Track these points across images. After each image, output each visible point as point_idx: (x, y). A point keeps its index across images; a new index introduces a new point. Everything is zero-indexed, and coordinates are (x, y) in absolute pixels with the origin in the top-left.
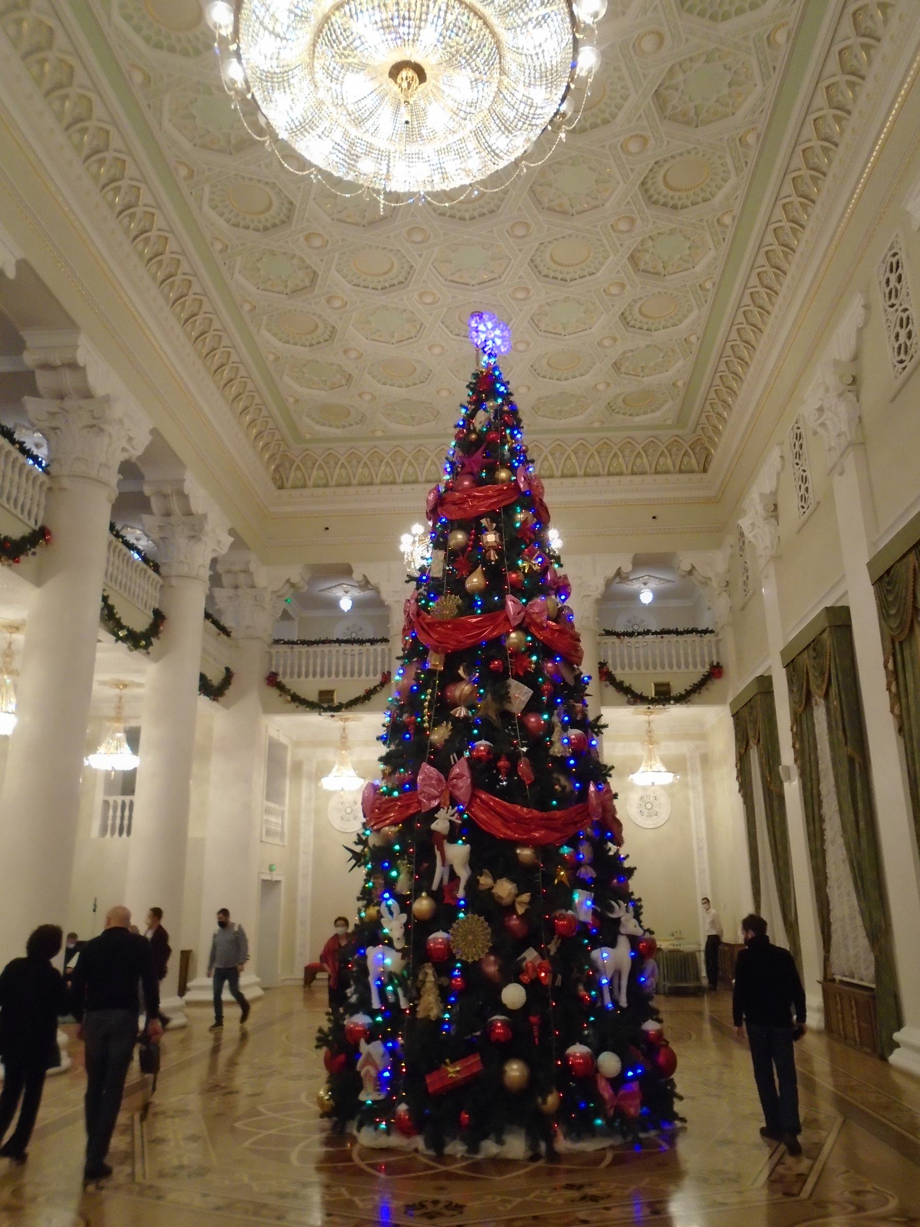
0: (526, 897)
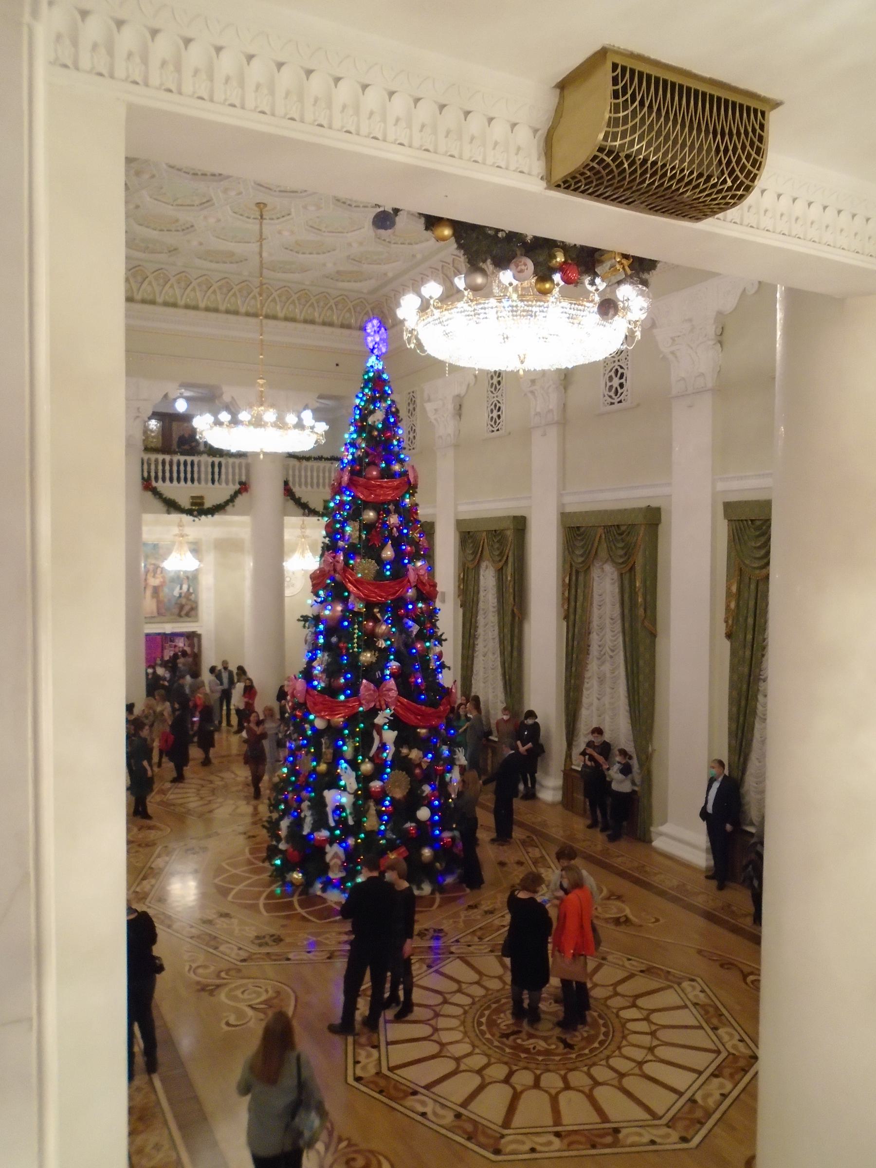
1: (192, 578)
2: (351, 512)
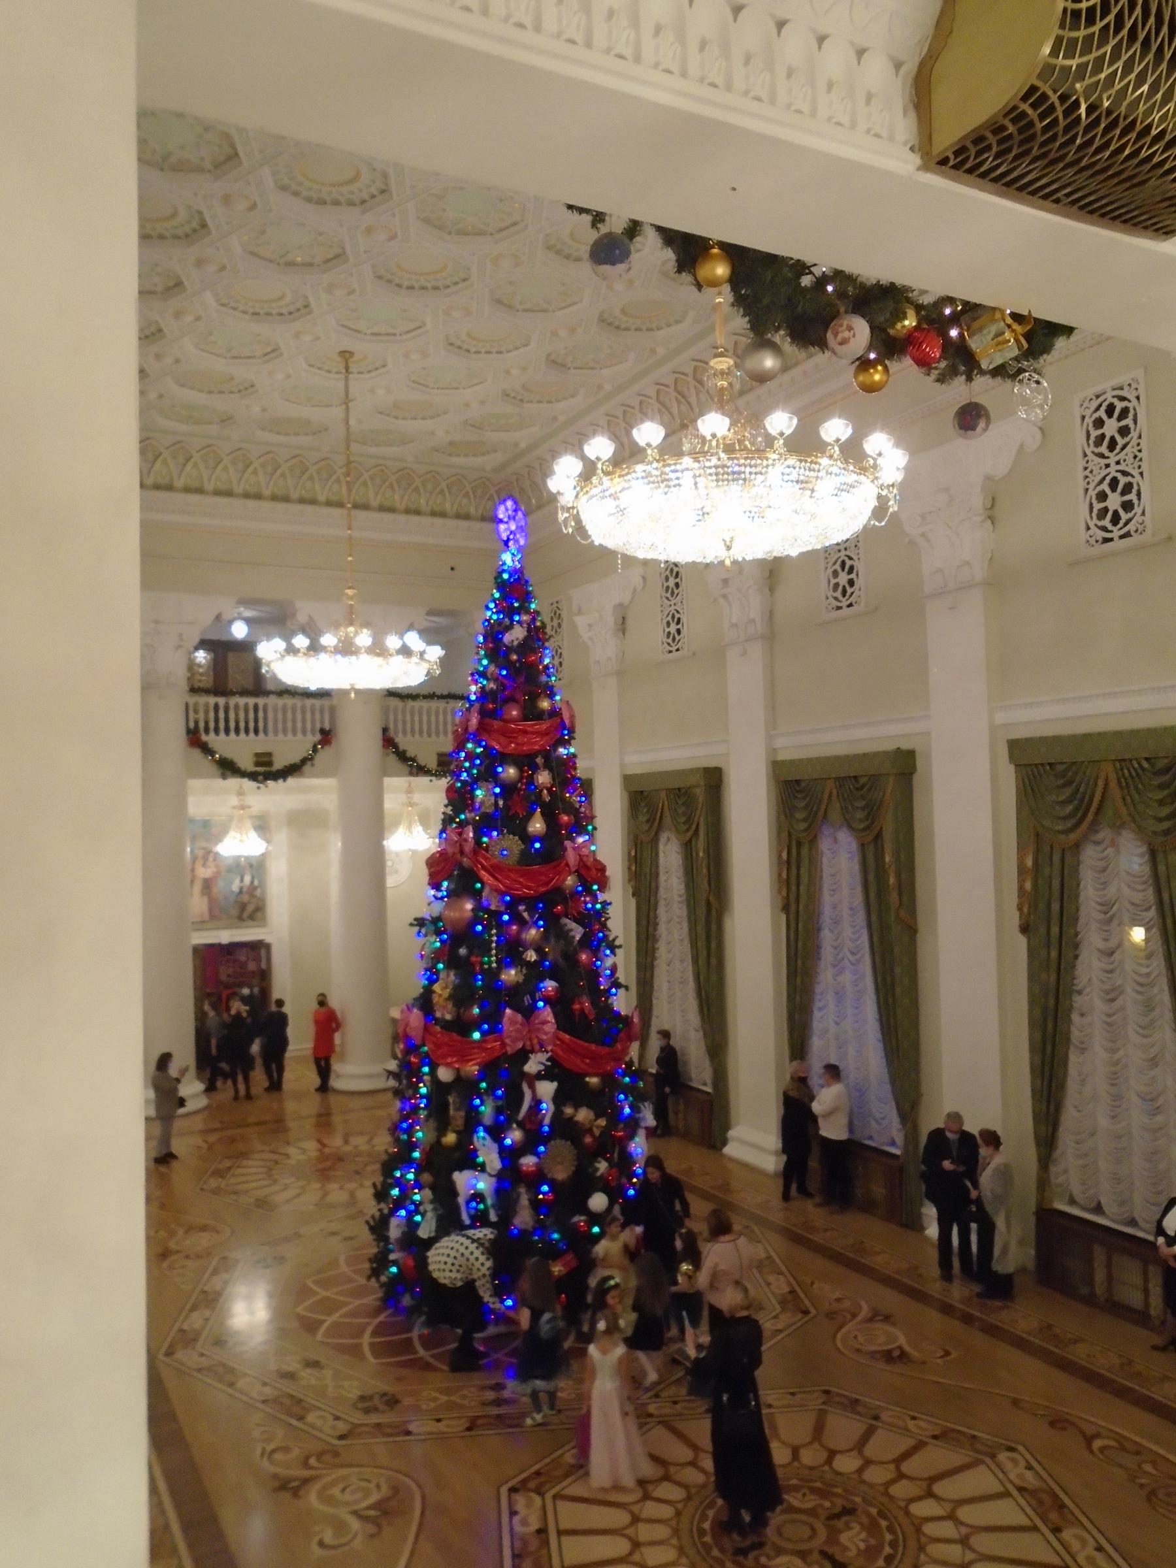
0: (602, 1122)
1: (257, 866)
2: (482, 768)
